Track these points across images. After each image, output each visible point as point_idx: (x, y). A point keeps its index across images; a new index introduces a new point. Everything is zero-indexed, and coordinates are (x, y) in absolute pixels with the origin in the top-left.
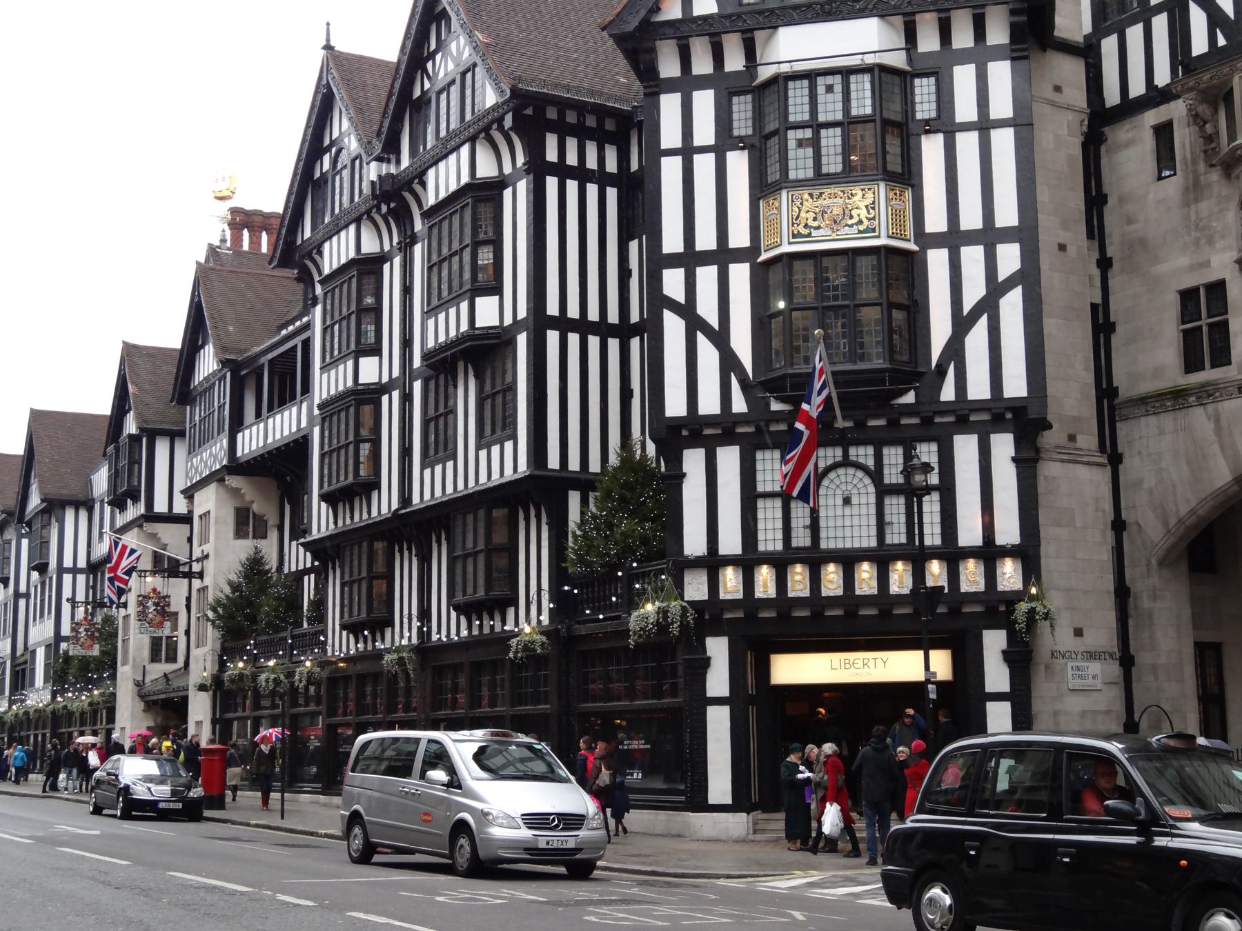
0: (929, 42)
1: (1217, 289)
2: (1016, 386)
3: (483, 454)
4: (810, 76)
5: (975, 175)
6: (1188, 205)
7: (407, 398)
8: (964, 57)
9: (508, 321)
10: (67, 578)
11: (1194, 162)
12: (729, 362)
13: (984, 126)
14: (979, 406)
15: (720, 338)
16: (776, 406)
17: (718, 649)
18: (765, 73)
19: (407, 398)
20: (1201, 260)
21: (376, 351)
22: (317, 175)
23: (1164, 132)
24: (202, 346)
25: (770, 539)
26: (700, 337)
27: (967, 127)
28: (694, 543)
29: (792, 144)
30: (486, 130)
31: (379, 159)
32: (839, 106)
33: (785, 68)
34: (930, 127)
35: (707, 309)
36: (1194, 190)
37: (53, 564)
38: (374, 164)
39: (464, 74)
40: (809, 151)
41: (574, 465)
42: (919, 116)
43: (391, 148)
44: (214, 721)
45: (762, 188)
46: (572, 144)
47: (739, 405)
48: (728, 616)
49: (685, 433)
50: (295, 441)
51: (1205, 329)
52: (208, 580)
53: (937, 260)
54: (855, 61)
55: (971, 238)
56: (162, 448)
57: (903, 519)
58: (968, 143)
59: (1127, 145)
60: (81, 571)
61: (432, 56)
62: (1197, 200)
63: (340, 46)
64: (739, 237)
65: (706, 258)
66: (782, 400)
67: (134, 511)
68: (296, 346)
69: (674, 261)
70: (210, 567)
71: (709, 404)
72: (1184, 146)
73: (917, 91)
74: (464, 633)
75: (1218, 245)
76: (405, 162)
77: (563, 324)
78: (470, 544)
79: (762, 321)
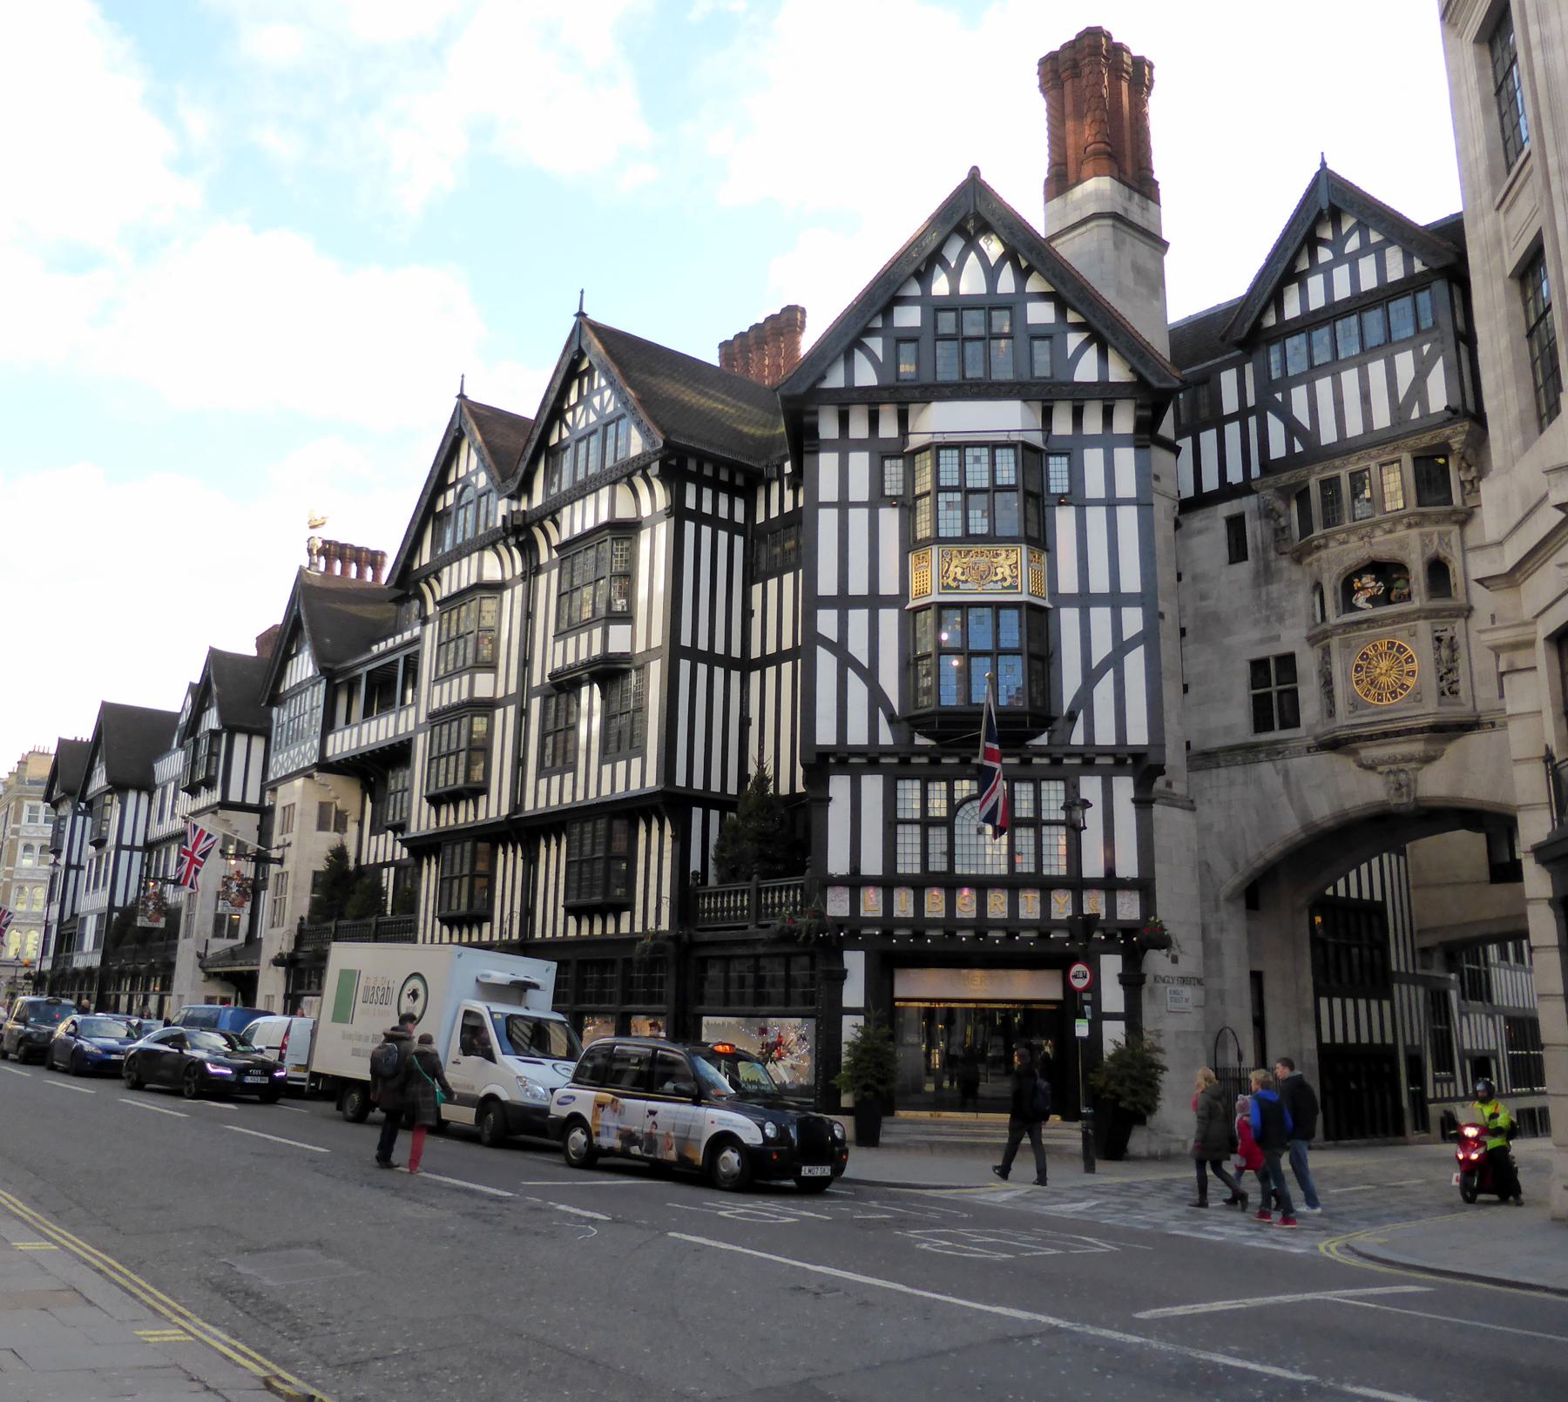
0: (1062, 425)
1: (1287, 662)
2: (1138, 735)
3: (607, 769)
4: (961, 447)
5: (1103, 542)
6: (1259, 586)
7: (523, 713)
8: (1093, 441)
9: (640, 648)
10: (125, 854)
11: (1265, 550)
12: (877, 698)
13: (1111, 503)
14: (1105, 751)
15: (870, 675)
16: (920, 741)
17: (855, 962)
18: (915, 441)
19: (523, 713)
20: (1273, 633)
21: (491, 667)
22: (440, 507)
23: (1236, 524)
24: (296, 655)
25: (908, 863)
26: (851, 673)
27: (1096, 502)
28: (838, 863)
29: (942, 506)
30: (630, 476)
31: (511, 497)
32: (986, 475)
33: (939, 439)
34: (1062, 500)
35: (858, 647)
36: (1265, 575)
37: (112, 841)
38: (505, 501)
39: (606, 425)
40: (959, 514)
41: (698, 784)
42: (1053, 490)
43: (526, 488)
44: (287, 997)
45: (910, 544)
46: (707, 494)
47: (886, 737)
48: (865, 932)
49: (832, 760)
50: (391, 746)
51: (1275, 695)
52: (287, 866)
53: (1069, 618)
54: (1002, 437)
55: (1100, 600)
56: (240, 741)
57: (1032, 850)
58: (1096, 516)
59: (1200, 532)
60: (138, 849)
61: (573, 408)
63: (473, 396)
64: (889, 586)
65: (858, 602)
66: (927, 735)
67: (208, 798)
68: (397, 661)
69: (828, 602)
70: (291, 855)
71: (858, 735)
73: (1051, 468)
74: (572, 932)
76: (538, 499)
77: (694, 655)
78: (587, 849)
79: (909, 664)
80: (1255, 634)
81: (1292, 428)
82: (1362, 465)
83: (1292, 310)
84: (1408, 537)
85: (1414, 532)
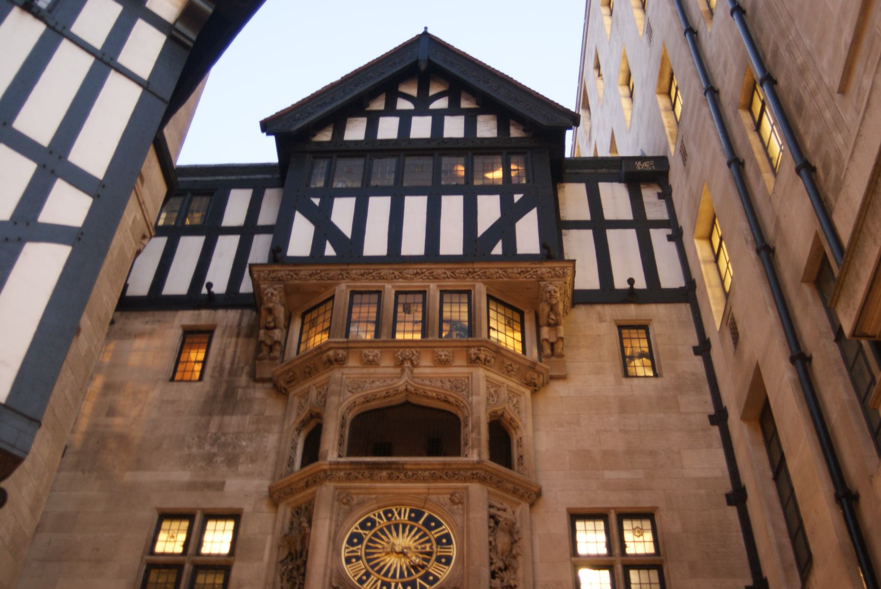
6: (210, 414)
11: (232, 373)
20: (211, 479)
36: (224, 399)
59: (140, 335)
62: (224, 412)
72: (224, 355)
75: (242, 468)
80: (184, 476)
81: (325, 230)
82: (417, 284)
83: (355, 131)
84: (470, 377)
85: (480, 373)
